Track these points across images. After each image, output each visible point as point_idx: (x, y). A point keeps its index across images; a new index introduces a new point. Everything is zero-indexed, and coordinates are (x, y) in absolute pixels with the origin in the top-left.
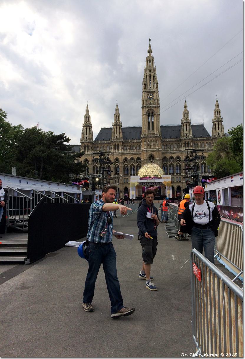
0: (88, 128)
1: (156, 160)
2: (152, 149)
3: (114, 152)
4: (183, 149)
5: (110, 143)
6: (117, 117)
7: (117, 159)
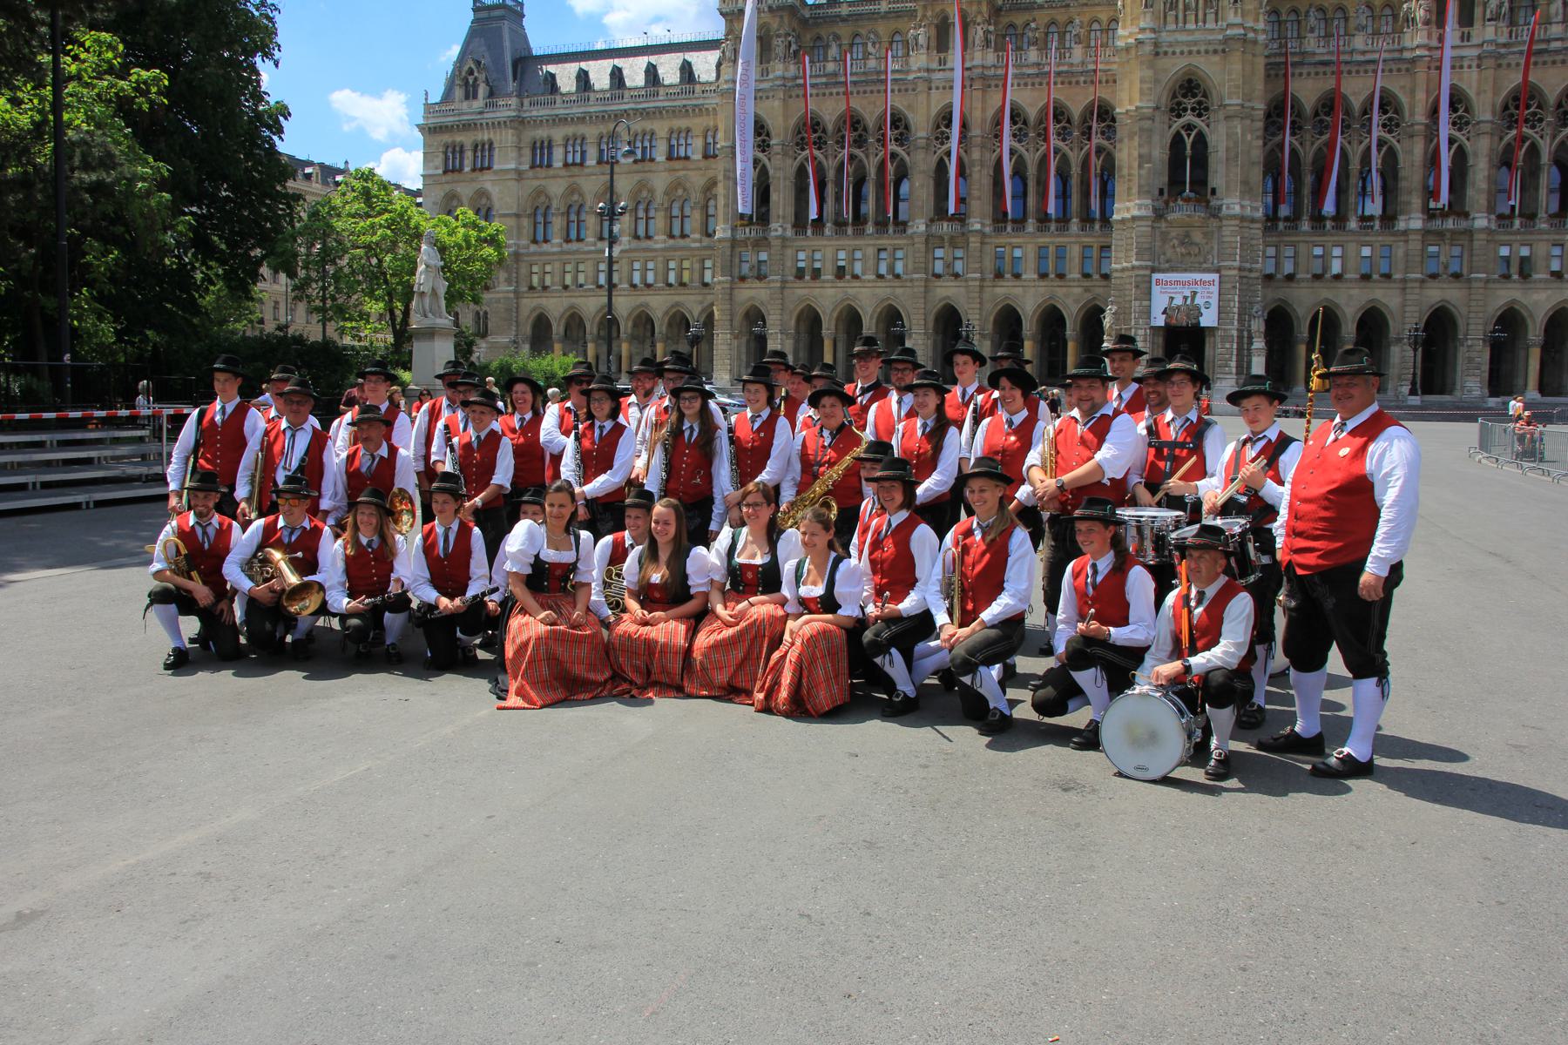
1: (1221, 115)
2: (1197, 36)
3: (935, 65)
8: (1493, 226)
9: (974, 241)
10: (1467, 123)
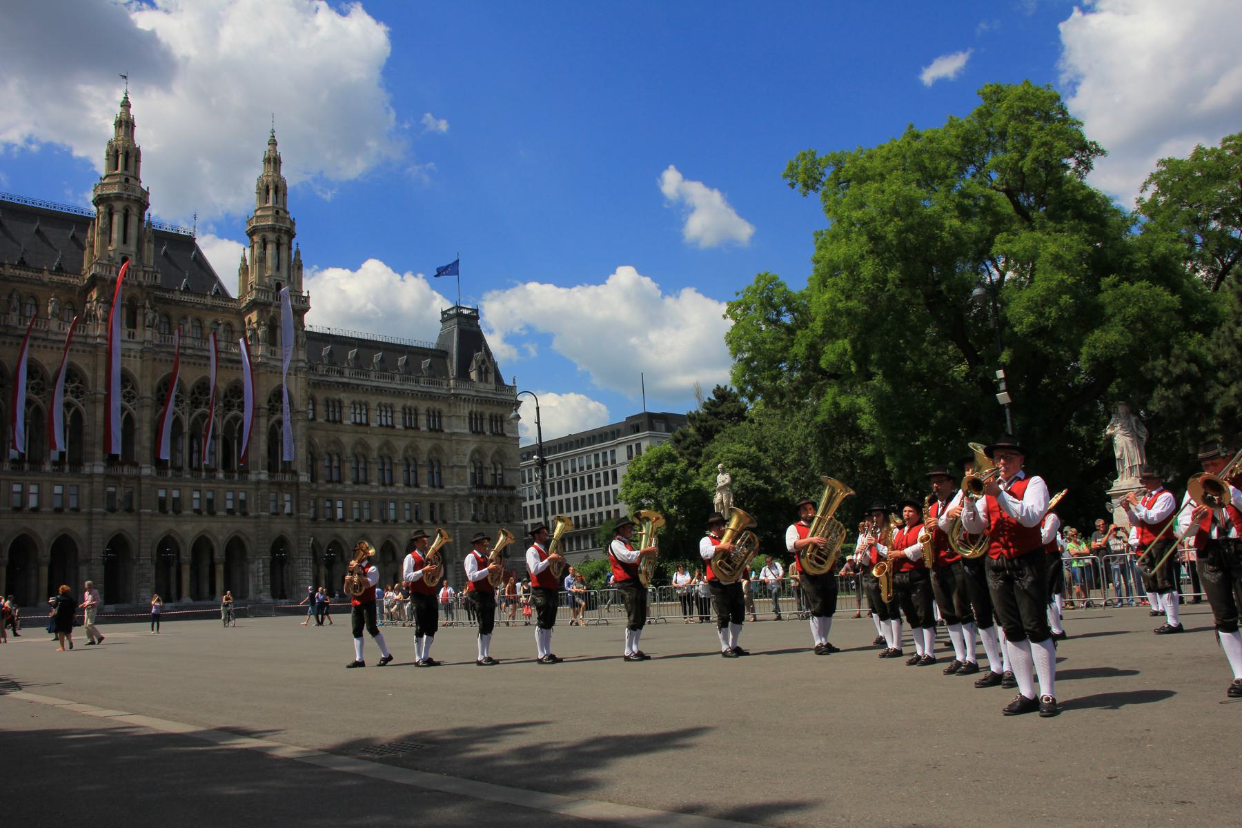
8: (154, 474)
10: (134, 397)
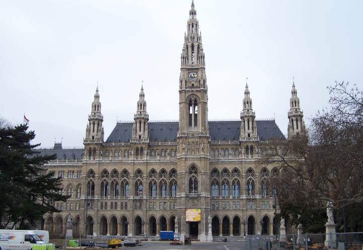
0: (96, 122)
1: (200, 174)
2: (195, 157)
3: (135, 159)
4: (243, 157)
5: (130, 146)
6: (141, 106)
7: (139, 172)
9: (145, 201)
